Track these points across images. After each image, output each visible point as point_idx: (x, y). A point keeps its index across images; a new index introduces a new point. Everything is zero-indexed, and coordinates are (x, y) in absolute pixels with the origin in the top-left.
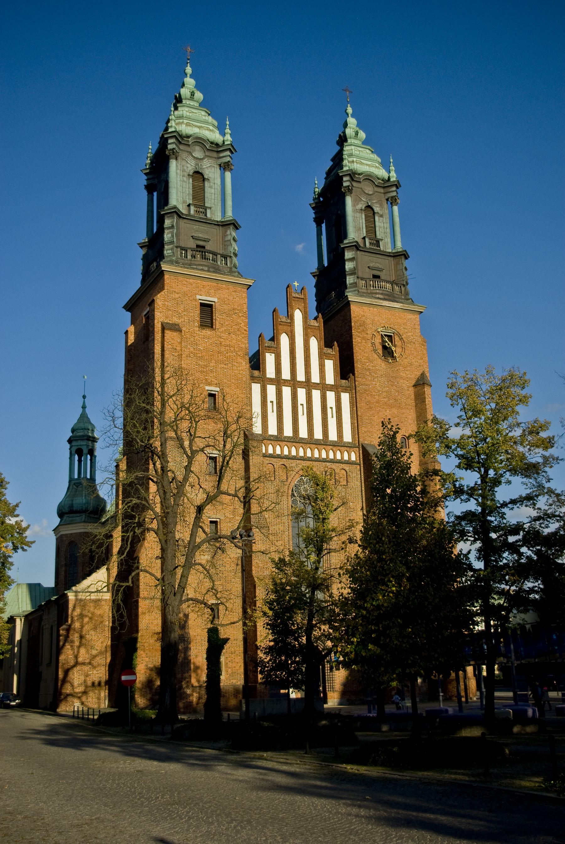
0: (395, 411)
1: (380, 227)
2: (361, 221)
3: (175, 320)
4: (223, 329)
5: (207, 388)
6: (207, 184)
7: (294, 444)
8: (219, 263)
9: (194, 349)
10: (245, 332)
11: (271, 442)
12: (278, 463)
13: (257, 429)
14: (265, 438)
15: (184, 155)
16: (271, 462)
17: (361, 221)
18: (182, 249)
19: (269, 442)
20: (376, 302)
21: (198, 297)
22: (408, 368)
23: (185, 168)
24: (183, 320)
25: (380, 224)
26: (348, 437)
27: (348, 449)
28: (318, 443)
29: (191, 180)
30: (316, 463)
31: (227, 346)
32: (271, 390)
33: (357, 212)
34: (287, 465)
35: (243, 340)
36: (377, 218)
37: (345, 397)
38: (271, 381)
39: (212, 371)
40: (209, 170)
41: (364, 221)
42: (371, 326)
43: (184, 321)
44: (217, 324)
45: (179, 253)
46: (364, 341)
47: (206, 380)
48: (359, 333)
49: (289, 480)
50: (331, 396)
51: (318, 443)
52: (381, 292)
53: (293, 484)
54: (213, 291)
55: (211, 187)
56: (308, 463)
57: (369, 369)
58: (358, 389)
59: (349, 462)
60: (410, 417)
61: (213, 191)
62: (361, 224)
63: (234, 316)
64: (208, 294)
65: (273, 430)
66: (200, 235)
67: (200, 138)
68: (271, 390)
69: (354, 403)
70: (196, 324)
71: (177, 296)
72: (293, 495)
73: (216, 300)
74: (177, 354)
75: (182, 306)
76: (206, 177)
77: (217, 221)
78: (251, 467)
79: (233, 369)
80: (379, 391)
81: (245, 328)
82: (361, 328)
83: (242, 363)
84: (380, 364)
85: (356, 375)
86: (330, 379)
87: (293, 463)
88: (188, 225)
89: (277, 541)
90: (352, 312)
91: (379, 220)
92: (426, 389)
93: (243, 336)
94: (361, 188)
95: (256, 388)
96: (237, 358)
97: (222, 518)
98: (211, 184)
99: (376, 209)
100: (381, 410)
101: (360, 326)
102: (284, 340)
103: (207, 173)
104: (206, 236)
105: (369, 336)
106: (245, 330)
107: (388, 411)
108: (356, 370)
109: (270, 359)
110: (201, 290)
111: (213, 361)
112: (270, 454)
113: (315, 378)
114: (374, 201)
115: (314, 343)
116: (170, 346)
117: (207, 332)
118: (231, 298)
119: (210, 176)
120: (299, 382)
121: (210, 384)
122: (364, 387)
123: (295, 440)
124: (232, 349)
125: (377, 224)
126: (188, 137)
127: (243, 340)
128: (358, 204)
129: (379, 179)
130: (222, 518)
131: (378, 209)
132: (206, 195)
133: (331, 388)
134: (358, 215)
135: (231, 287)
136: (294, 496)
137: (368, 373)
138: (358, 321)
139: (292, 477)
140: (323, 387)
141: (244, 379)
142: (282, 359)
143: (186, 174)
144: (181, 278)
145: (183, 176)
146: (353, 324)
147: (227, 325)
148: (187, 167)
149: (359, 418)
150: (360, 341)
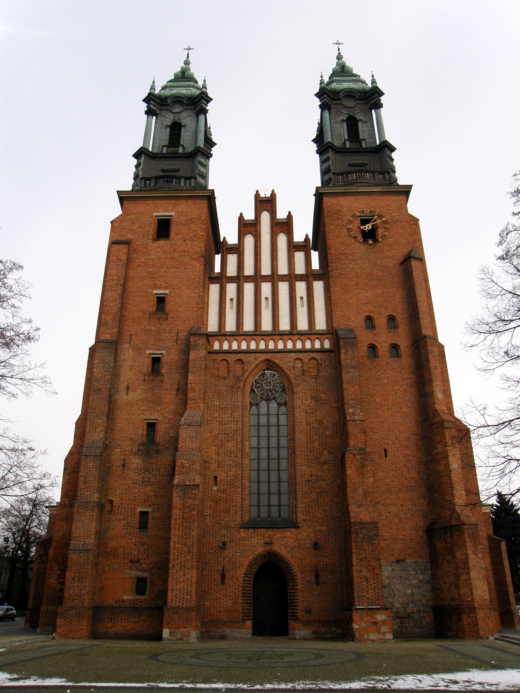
0: (379, 291)
1: (363, 131)
2: (342, 130)
3: (130, 236)
4: (178, 238)
5: (155, 292)
6: (183, 130)
7: (253, 337)
8: (182, 184)
9: (146, 259)
10: (201, 237)
11: (226, 338)
12: (232, 359)
13: (213, 326)
14: (222, 334)
15: (164, 113)
16: (224, 358)
17: (342, 130)
18: (146, 179)
19: (224, 338)
20: (351, 189)
21: (155, 214)
22: (394, 247)
23: (164, 122)
24: (137, 235)
25: (364, 129)
26: (321, 324)
27: (319, 336)
28: (282, 335)
29: (168, 130)
30: (280, 354)
31: (181, 252)
33: (338, 123)
34: (244, 360)
35: (199, 244)
36: (360, 125)
37: (318, 286)
38: (231, 280)
39: (162, 276)
40: (187, 119)
41: (346, 129)
42: (347, 212)
43: (138, 236)
44: (172, 234)
45: (143, 183)
46: (338, 228)
47: (155, 285)
48: (333, 220)
49: (246, 374)
50: (301, 287)
51: (282, 335)
52: (360, 181)
53: (251, 380)
54: (171, 207)
55: (187, 131)
56: (269, 356)
57: (345, 254)
58: (331, 274)
59: (323, 351)
60: (398, 296)
61: (189, 134)
62: (342, 132)
63: (191, 225)
65: (230, 326)
66: (170, 168)
67: (179, 97)
69: (327, 290)
71: (133, 216)
72: (252, 390)
73: (173, 214)
74: (122, 263)
75: (138, 224)
76: (183, 124)
77: (187, 153)
78: (191, 362)
79: (185, 272)
80: (357, 273)
81: (202, 233)
82: (335, 216)
83: (196, 265)
84: (360, 249)
85: (329, 261)
87: (252, 357)
88: (161, 163)
89: (228, 441)
90: (324, 203)
91: (362, 126)
92: (412, 263)
93: (199, 240)
94: (342, 104)
95: (214, 289)
96: (191, 261)
97: (159, 419)
98: (188, 129)
99: (358, 118)
100: (361, 291)
101: (334, 214)
102: (249, 240)
103: (184, 122)
104: (176, 167)
105: (344, 223)
106: (202, 235)
107: (369, 293)
108: (329, 256)
110: (159, 208)
111: (165, 267)
112: (225, 350)
113: (283, 269)
114: (357, 112)
115: (282, 239)
116: (114, 258)
117: (162, 242)
118: (189, 210)
119: (187, 123)
120: (263, 276)
122: (338, 271)
123: (257, 334)
124: (186, 254)
125: (360, 129)
126: (167, 98)
127: (199, 244)
128: (338, 117)
129: (360, 92)
130: (160, 418)
131: (361, 117)
132: (182, 137)
133: (301, 278)
134: (339, 125)
135: (190, 202)
136: (254, 392)
137: (344, 257)
138: (332, 210)
139: (249, 371)
140: (292, 278)
141: (197, 280)
142: (245, 257)
143: (164, 126)
144: (139, 202)
145: (162, 128)
146: (326, 214)
147: (183, 233)
148: (166, 121)
149: (333, 302)
150: (333, 228)
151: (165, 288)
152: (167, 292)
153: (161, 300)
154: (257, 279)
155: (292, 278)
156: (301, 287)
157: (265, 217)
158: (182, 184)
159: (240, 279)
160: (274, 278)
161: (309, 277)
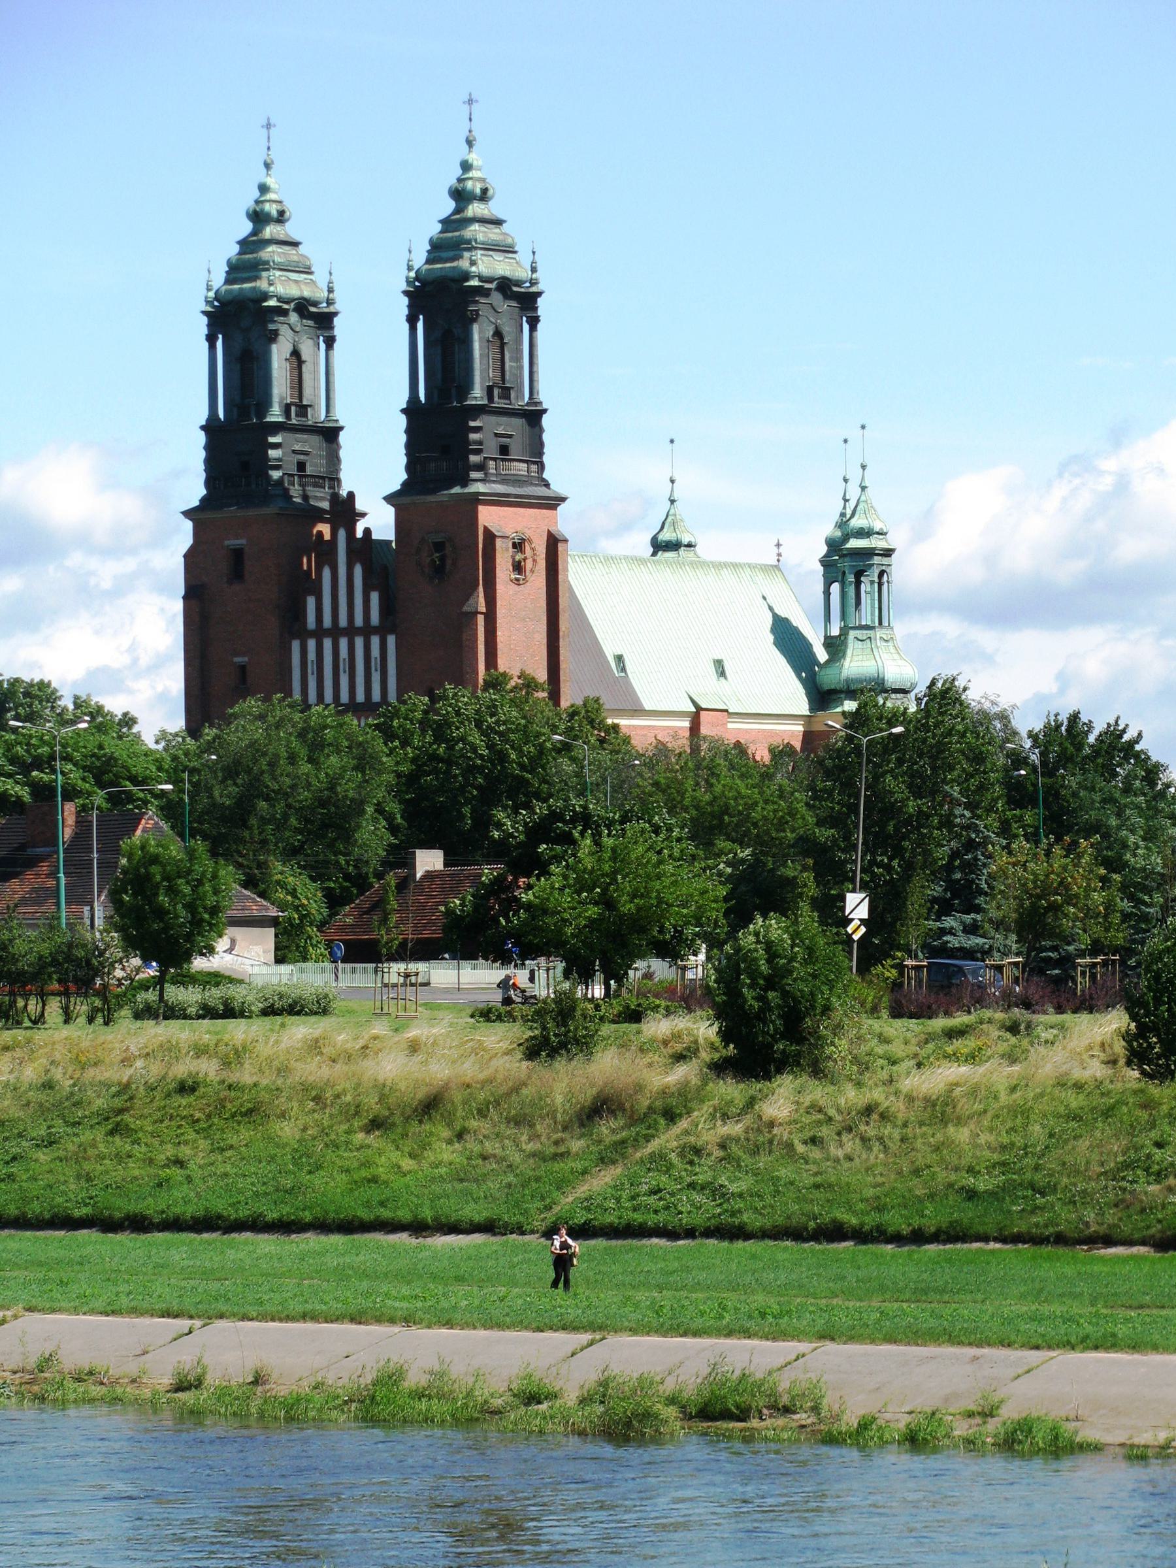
8: (254, 486)
21: (227, 543)
32: (312, 644)
37: (391, 640)
38: (312, 634)
50: (375, 641)
64: (237, 537)
68: (312, 644)
70: (225, 579)
73: (243, 541)
86: (375, 619)
95: (296, 645)
102: (327, 573)
109: (311, 602)
115: (358, 570)
121: (238, 655)
151: (243, 654)
152: (246, 659)
153: (243, 668)
154: (335, 632)
155: (367, 631)
156: (375, 641)
157: (342, 534)
158: (254, 486)
159: (319, 633)
160: (351, 632)
161: (382, 631)
